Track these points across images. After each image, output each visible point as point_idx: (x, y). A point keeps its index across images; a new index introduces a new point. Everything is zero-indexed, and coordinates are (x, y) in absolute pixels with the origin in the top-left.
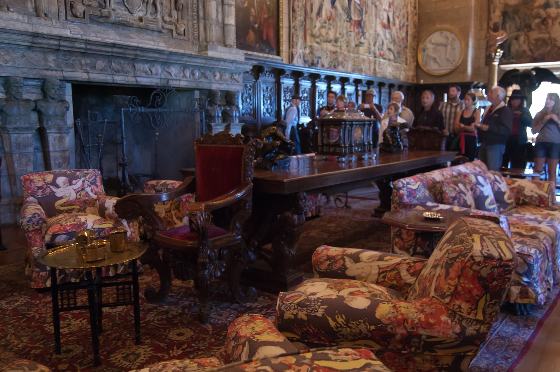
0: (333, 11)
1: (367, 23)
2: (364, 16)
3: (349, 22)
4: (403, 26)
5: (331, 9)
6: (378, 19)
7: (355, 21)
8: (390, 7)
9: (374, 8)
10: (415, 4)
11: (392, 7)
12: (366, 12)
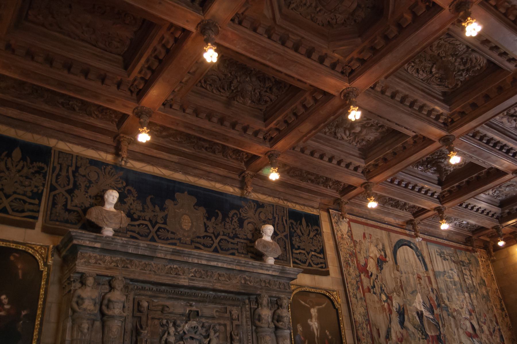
0: (404, 332)
1: (448, 336)
2: (441, 329)
3: (426, 339)
4: (494, 331)
5: (401, 330)
6: (460, 329)
7: (432, 336)
8: (471, 314)
9: (452, 319)
10: (501, 305)
11: (473, 314)
12: (444, 325)
